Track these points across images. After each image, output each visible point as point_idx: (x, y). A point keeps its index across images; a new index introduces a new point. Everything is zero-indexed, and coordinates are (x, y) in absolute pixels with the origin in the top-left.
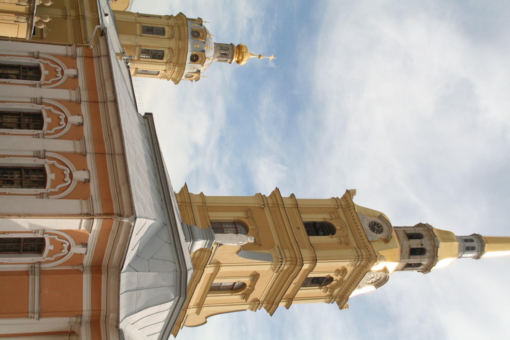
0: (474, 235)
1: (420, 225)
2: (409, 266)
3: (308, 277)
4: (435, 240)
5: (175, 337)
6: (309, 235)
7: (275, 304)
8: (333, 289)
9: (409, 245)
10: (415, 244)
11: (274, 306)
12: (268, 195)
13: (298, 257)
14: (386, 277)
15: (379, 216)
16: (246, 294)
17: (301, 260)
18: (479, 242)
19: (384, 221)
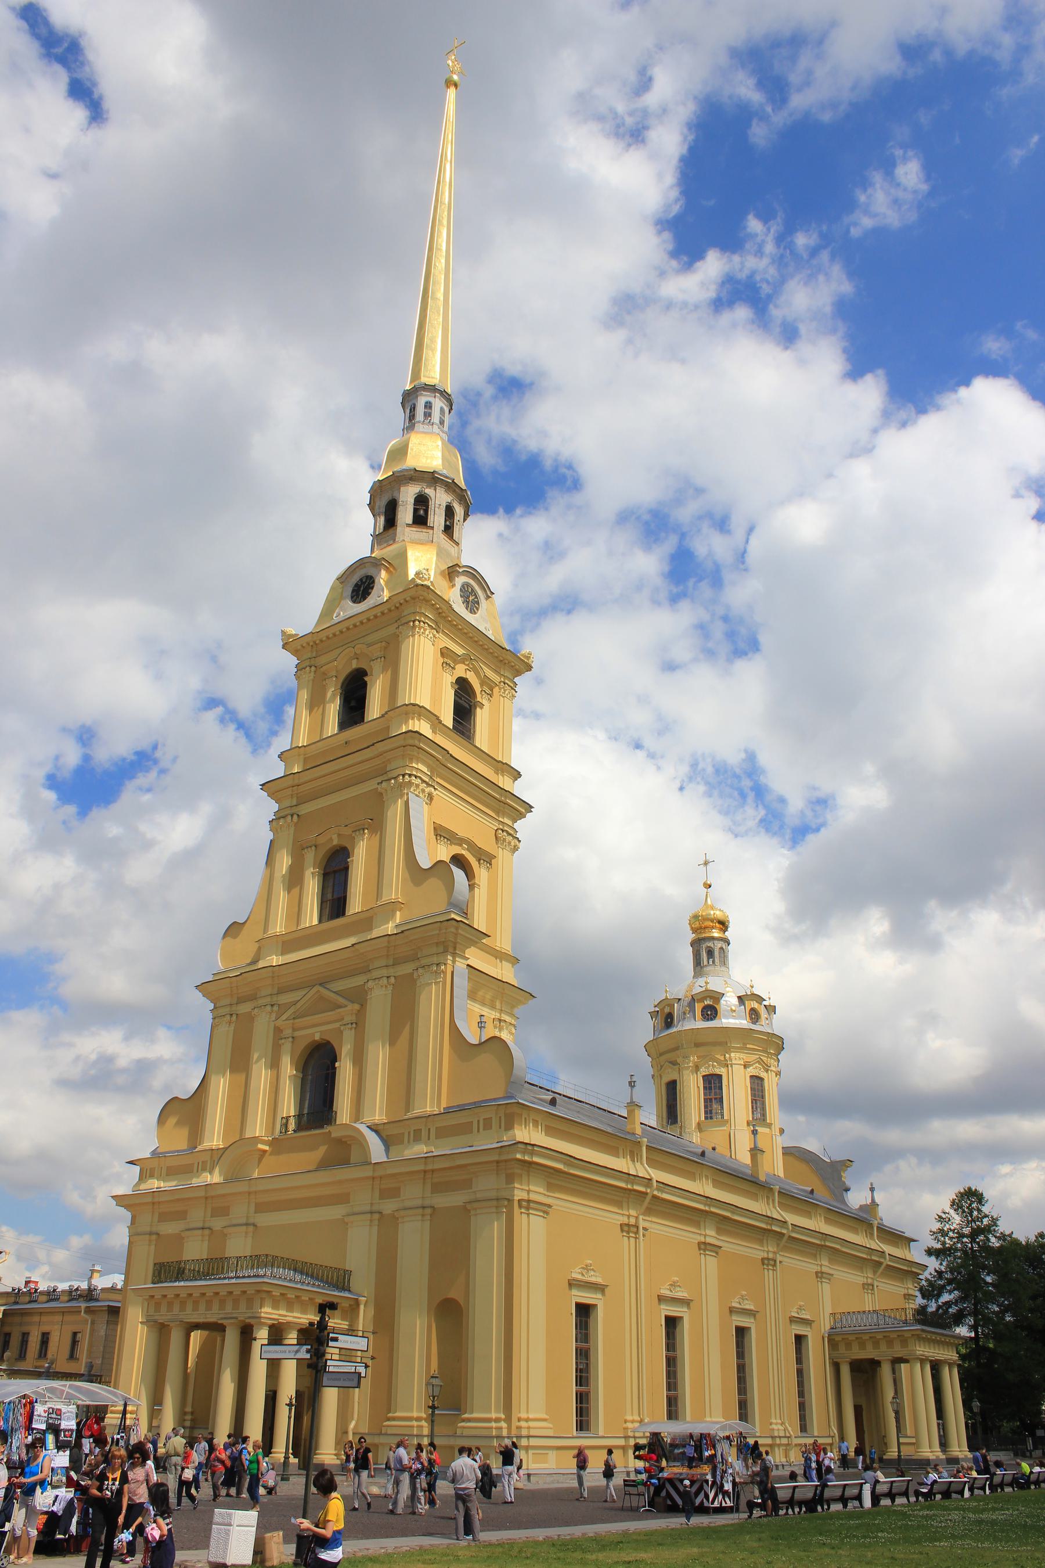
0: (403, 404)
1: (371, 506)
6: (363, 721)
7: (506, 798)
8: (485, 681)
10: (405, 514)
13: (402, 743)
15: (342, 583)
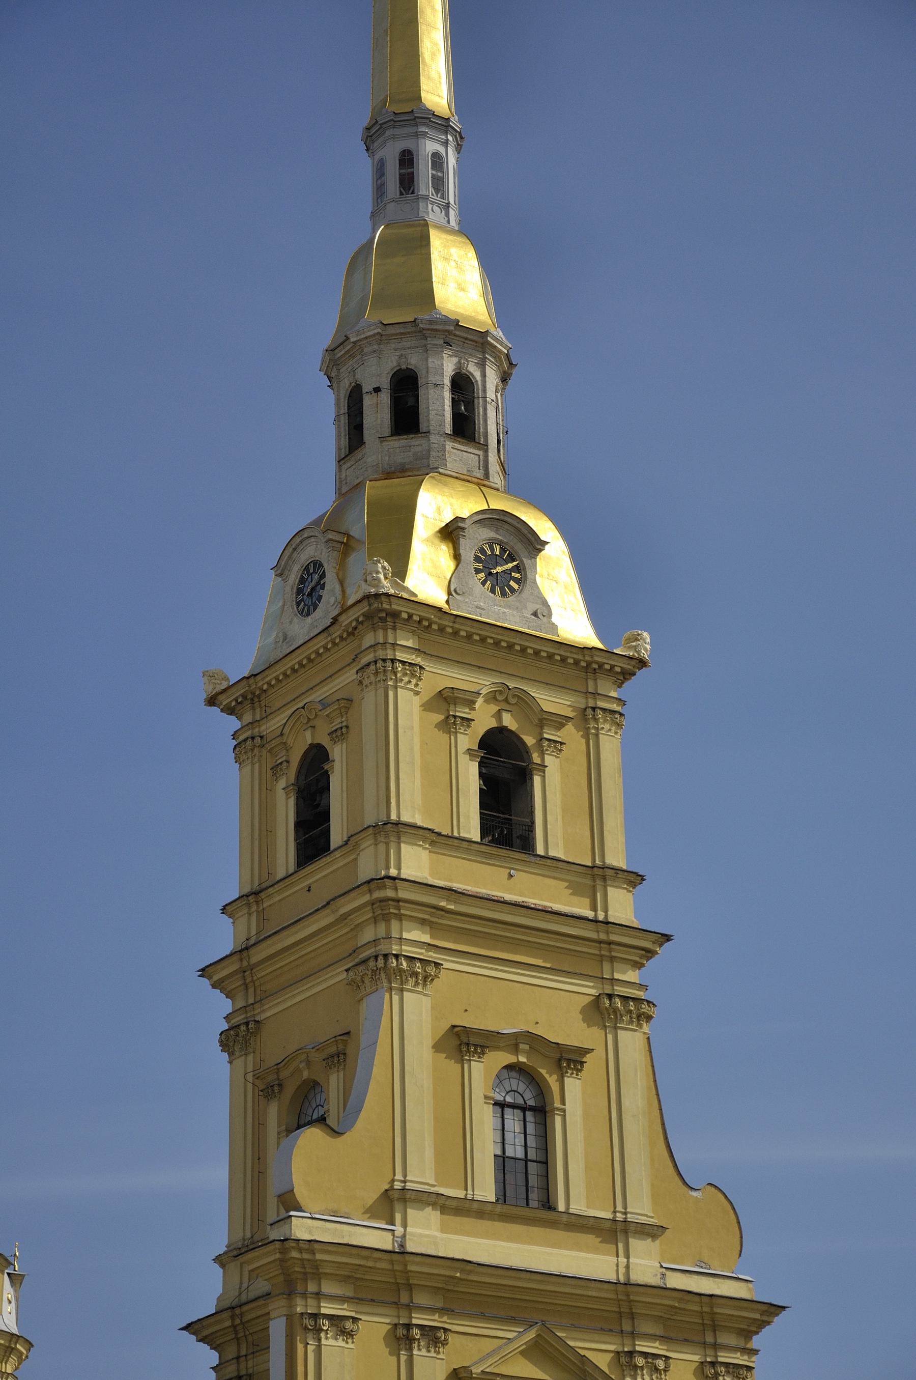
4: (360, 340)
5: (784, 1308)
7: (608, 933)
9: (378, 440)
11: (613, 938)
12: (226, 1006)
13: (366, 898)
14: (487, 522)
15: (280, 575)
16: (558, 1056)
17: (373, 885)
18: (381, 139)
19: (290, 557)
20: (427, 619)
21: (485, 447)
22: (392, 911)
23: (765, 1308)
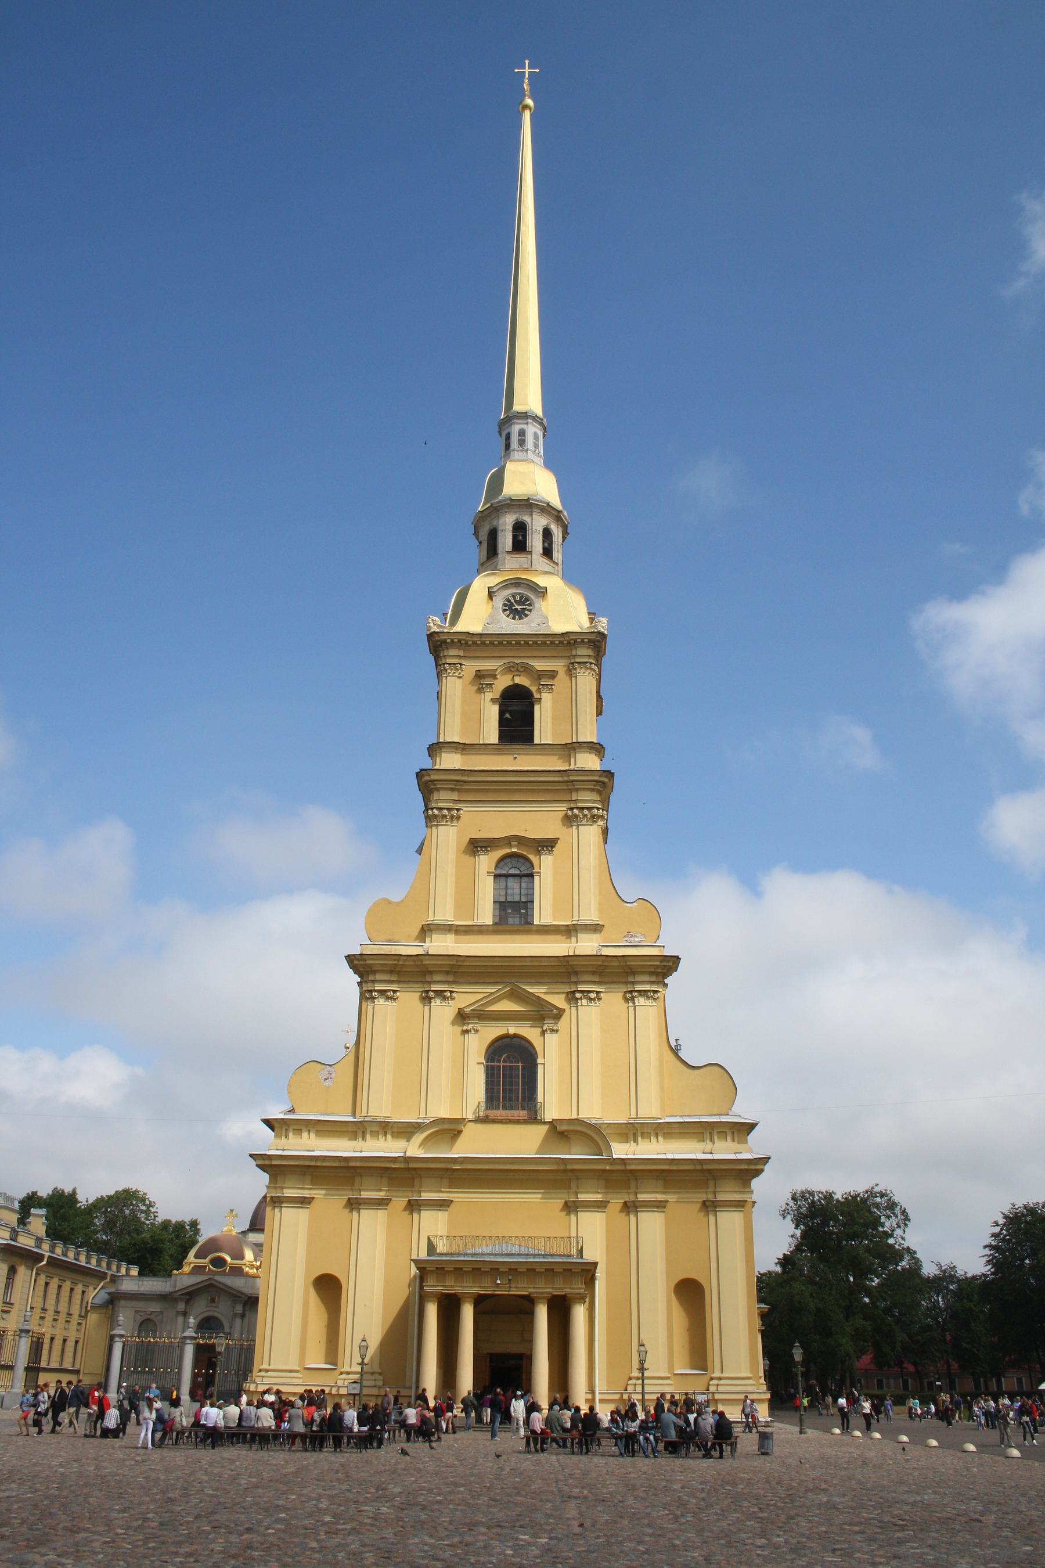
2: (520, 546)
3: (496, 742)
7: (568, 776)
8: (539, 676)
11: (572, 778)
20: (463, 640)
21: (531, 553)
22: (432, 787)
23: (661, 958)
